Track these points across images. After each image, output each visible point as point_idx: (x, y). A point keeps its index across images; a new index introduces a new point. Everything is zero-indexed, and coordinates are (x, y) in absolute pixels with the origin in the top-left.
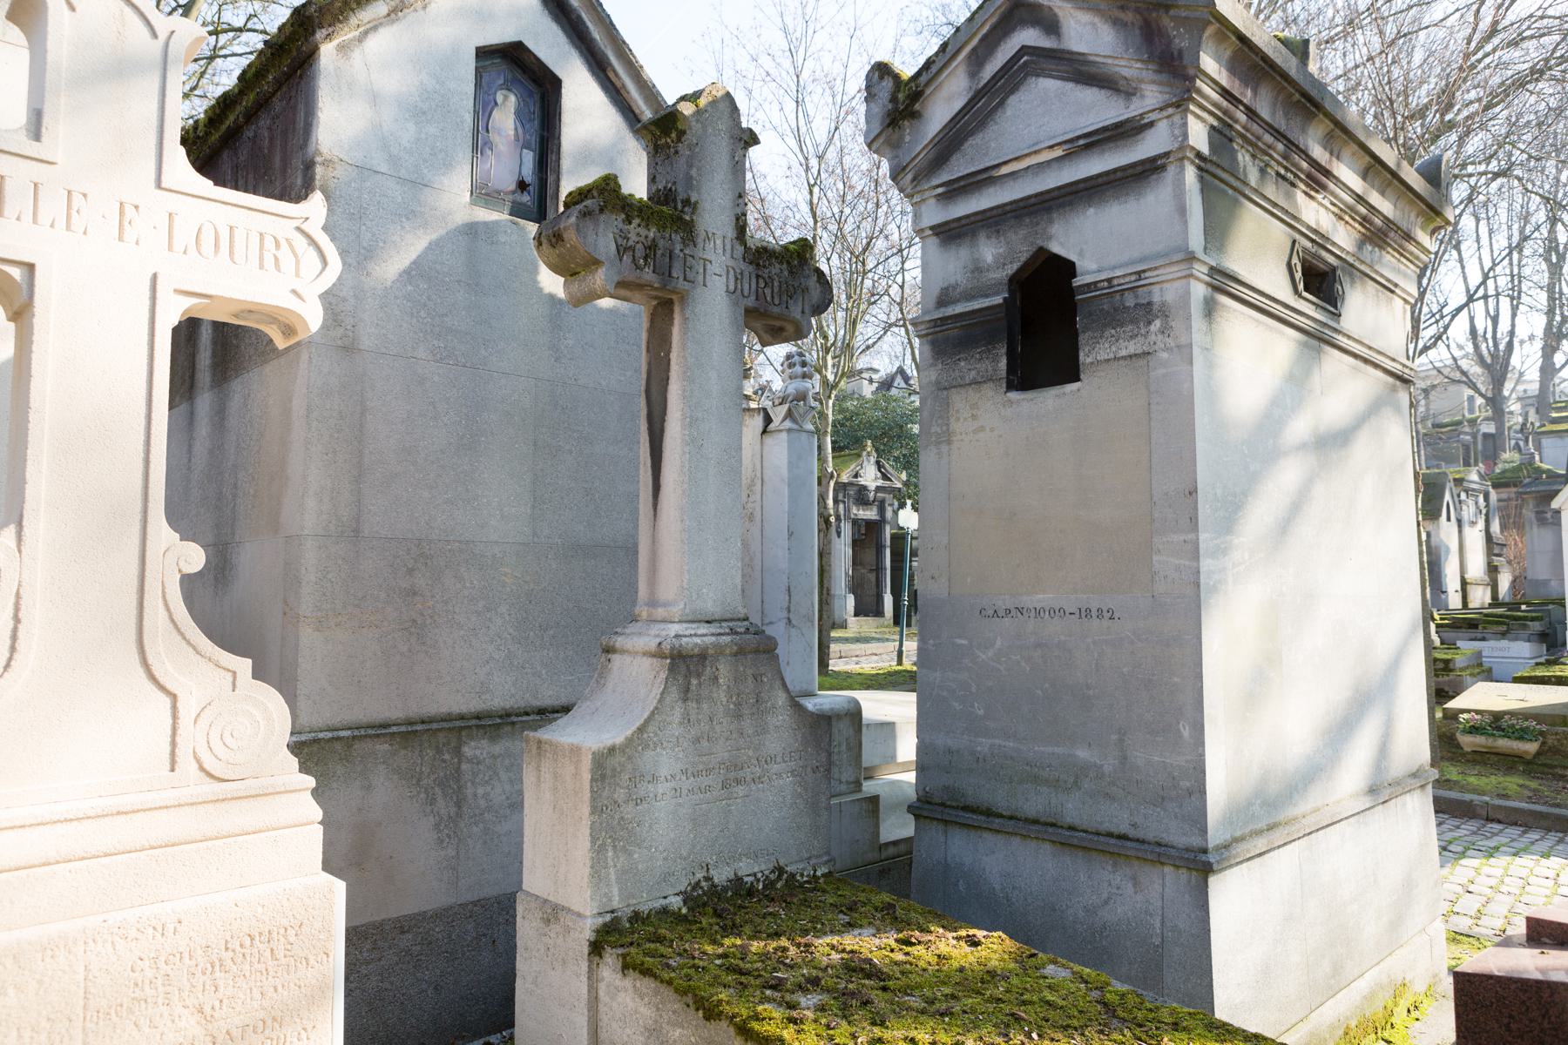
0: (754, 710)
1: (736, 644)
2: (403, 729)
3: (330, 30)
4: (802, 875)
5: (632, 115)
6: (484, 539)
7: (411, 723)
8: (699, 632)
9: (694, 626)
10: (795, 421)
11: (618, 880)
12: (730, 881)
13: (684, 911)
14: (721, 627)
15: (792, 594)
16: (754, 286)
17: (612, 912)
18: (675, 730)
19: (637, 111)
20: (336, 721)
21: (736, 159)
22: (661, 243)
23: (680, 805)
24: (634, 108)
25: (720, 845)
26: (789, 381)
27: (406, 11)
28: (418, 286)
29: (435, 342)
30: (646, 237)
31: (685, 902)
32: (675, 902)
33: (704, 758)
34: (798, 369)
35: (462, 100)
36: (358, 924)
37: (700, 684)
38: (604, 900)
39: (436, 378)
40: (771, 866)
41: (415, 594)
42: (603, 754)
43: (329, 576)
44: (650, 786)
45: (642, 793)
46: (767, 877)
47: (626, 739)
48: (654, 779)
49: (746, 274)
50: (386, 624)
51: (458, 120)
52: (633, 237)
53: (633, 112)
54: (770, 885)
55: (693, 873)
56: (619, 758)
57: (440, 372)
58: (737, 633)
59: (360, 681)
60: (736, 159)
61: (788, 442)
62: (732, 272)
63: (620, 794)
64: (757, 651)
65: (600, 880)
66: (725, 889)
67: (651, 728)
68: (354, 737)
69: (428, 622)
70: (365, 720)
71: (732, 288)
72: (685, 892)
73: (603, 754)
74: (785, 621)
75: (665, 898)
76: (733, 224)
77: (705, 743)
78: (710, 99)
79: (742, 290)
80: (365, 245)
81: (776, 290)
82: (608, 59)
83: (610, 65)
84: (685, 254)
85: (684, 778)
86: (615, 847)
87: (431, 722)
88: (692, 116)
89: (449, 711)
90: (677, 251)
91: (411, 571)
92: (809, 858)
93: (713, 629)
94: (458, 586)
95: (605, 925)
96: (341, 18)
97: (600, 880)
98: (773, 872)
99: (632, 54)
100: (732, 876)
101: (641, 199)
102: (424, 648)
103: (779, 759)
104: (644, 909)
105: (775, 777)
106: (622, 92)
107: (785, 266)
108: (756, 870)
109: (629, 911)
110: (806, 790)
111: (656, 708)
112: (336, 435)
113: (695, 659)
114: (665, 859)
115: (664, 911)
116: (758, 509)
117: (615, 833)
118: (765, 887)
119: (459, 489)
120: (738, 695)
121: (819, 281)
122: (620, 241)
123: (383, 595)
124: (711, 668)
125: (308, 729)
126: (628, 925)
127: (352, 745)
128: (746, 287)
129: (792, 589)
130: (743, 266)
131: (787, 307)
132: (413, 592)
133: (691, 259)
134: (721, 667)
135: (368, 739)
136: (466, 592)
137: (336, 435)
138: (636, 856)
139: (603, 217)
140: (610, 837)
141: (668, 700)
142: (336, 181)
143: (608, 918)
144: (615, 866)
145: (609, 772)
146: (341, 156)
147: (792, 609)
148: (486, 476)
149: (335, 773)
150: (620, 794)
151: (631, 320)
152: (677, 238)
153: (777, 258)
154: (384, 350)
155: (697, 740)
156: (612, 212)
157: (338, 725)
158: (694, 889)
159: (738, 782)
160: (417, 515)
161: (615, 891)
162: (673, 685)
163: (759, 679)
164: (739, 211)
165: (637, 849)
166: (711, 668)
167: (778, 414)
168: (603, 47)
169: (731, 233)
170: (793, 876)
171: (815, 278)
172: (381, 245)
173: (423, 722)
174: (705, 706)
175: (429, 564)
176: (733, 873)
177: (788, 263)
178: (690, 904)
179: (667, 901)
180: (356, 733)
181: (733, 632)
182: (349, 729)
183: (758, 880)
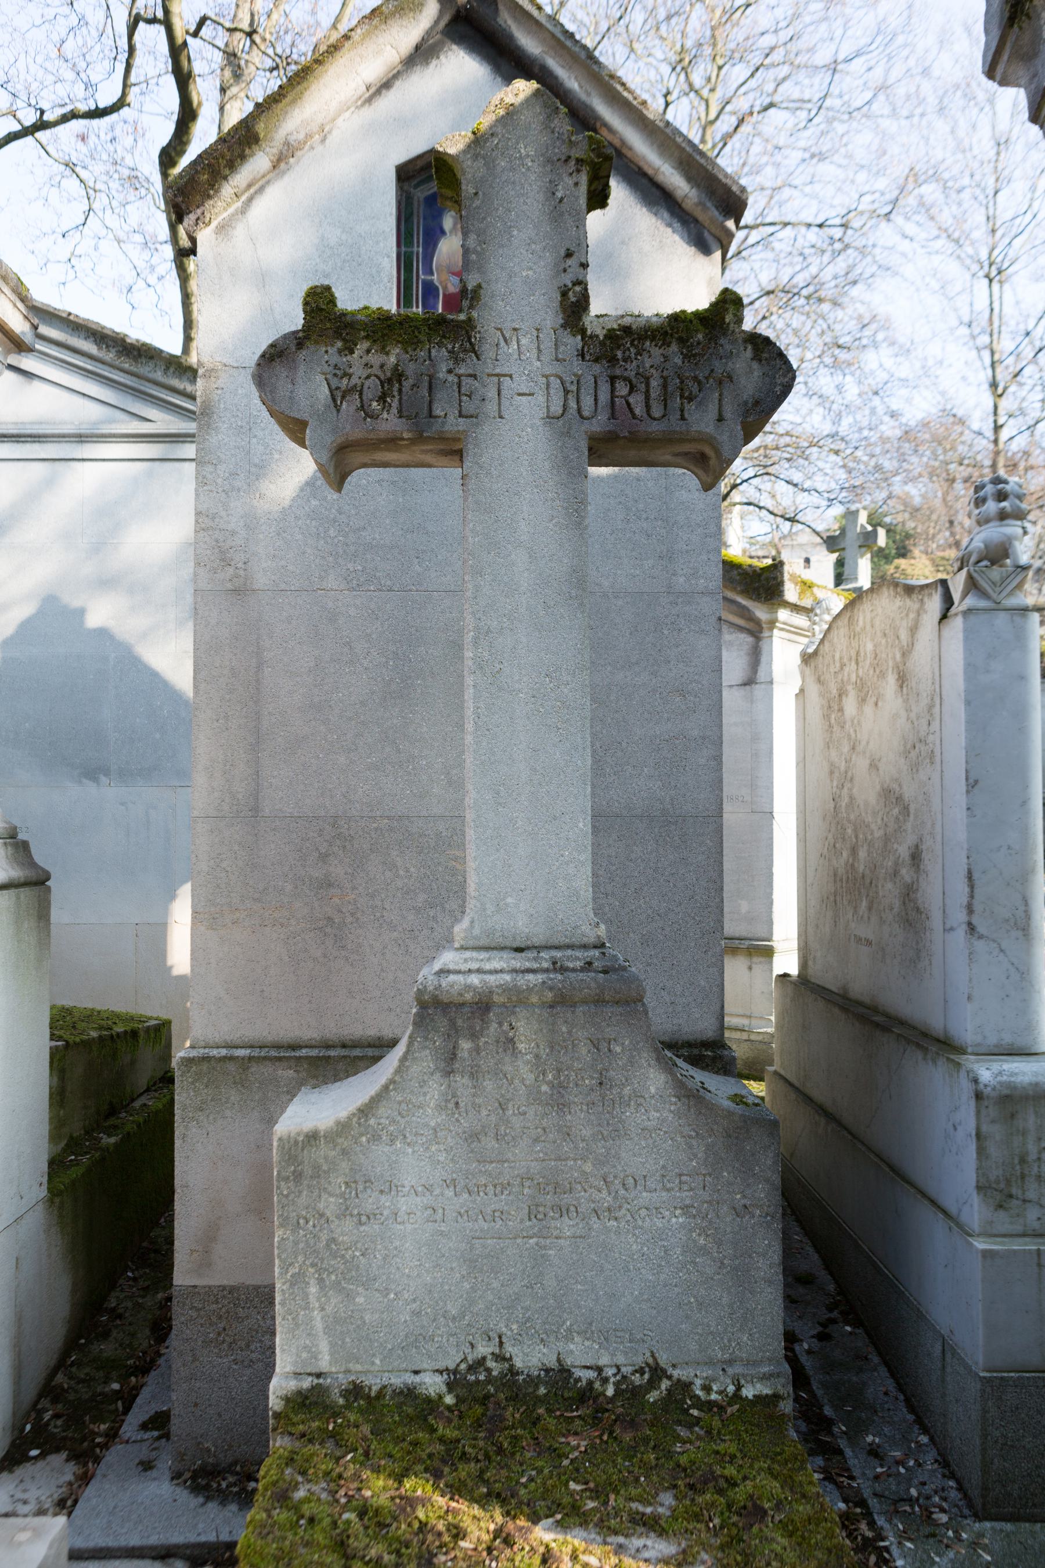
0: (595, 1096)
1: (551, 989)
2: (314, 1053)
3: (199, 211)
4: (707, 1389)
5: (644, 181)
6: (424, 813)
7: (328, 1047)
8: (488, 966)
9: (483, 955)
10: (984, 594)
11: (327, 1330)
12: (547, 1371)
13: (449, 1400)
14: (535, 959)
15: (977, 883)
16: (604, 396)
17: (319, 1375)
18: (430, 1115)
19: (650, 172)
20: (235, 1037)
21: (559, 195)
22: (410, 369)
23: (442, 1233)
24: (646, 168)
25: (527, 1309)
26: (978, 529)
27: (299, 153)
28: (325, 499)
29: (350, 566)
30: (382, 366)
31: (450, 1386)
32: (432, 1384)
33: (490, 1167)
34: (992, 507)
35: (377, 243)
36: (259, 1283)
37: (477, 1050)
38: (304, 1355)
39: (352, 612)
40: (639, 1361)
41: (330, 885)
42: (296, 1142)
43: (224, 865)
44: (383, 1198)
45: (369, 1206)
46: (624, 1377)
47: (338, 1123)
48: (391, 1187)
49: (588, 381)
50: (293, 922)
51: (374, 271)
52: (358, 372)
53: (645, 175)
54: (630, 1393)
55: (472, 1346)
56: (322, 1152)
57: (358, 602)
58: (563, 969)
59: (263, 991)
60: (559, 195)
61: (965, 630)
62: (555, 383)
63: (329, 1205)
64: (599, 1001)
65: (297, 1325)
66: (533, 1381)
67: (383, 1111)
68: (251, 1058)
69: (349, 920)
70: (270, 1039)
71: (557, 408)
72: (455, 1372)
73: (296, 1142)
74: (964, 927)
75: (416, 1372)
76: (556, 304)
77: (490, 1143)
78: (502, 112)
79: (579, 410)
80: (257, 461)
81: (654, 394)
82: (593, 111)
83: (597, 118)
84: (459, 376)
85: (449, 1193)
86: (321, 1281)
87: (355, 1047)
88: (466, 151)
89: (378, 1034)
90: (441, 375)
91: (324, 857)
92: (730, 1362)
93: (518, 962)
94: (388, 874)
95: (299, 1392)
96: (212, 192)
97: (297, 1325)
98: (641, 1371)
99: (627, 89)
100: (551, 1362)
101: (388, 311)
102: (343, 953)
103: (651, 1184)
104: (374, 1383)
105: (643, 1212)
106: (624, 151)
107: (674, 347)
108: (604, 1361)
109: (344, 1380)
110: (719, 1243)
111: (392, 1081)
112: (228, 697)
113: (466, 1009)
114: (417, 1314)
115: (409, 1393)
116: (938, 742)
117: (322, 1260)
118: (618, 1392)
119: (387, 749)
120: (559, 1071)
121: (757, 357)
122: (335, 383)
123: (289, 887)
124: (500, 1024)
125: (203, 1044)
126: (341, 1401)
127: (248, 1068)
128: (587, 402)
129: (976, 876)
130: (577, 367)
131: (683, 418)
132: (327, 883)
133: (470, 380)
134: (521, 1025)
135: (267, 1063)
136: (400, 884)
137: (228, 697)
138: (360, 1300)
139: (303, 354)
140: (313, 1265)
141: (415, 1069)
142: (219, 392)
143: (306, 1383)
144: (323, 1309)
145: (308, 1171)
146: (224, 361)
147: (978, 907)
148: (425, 729)
149: (228, 1099)
150: (329, 1205)
151: (650, 484)
152: (440, 354)
153: (653, 339)
154: (283, 586)
155: (473, 1137)
156: (316, 342)
157: (239, 1042)
158: (471, 1368)
159: (562, 1211)
160: (330, 786)
161: (324, 1346)
162: (425, 1047)
163: (604, 1046)
164: (567, 279)
165: (360, 1289)
166: (500, 1024)
167: (957, 585)
168: (583, 97)
169: (550, 318)
170: (685, 1386)
171: (749, 353)
172: (276, 456)
173: (344, 1046)
174: (488, 1084)
175: (348, 847)
176: (555, 1358)
177: (682, 341)
178: (463, 1392)
179: (417, 1379)
180: (256, 1053)
181: (557, 967)
182: (251, 1047)
183: (605, 1381)
